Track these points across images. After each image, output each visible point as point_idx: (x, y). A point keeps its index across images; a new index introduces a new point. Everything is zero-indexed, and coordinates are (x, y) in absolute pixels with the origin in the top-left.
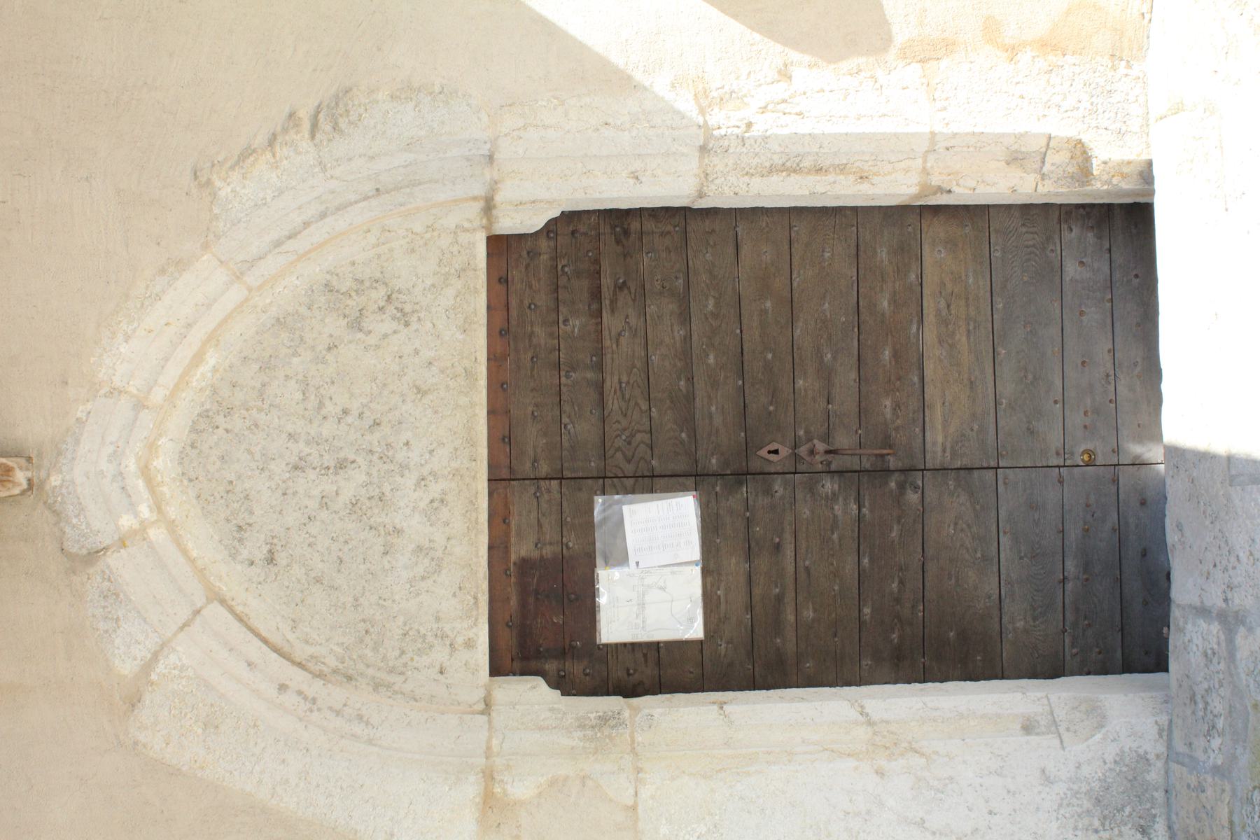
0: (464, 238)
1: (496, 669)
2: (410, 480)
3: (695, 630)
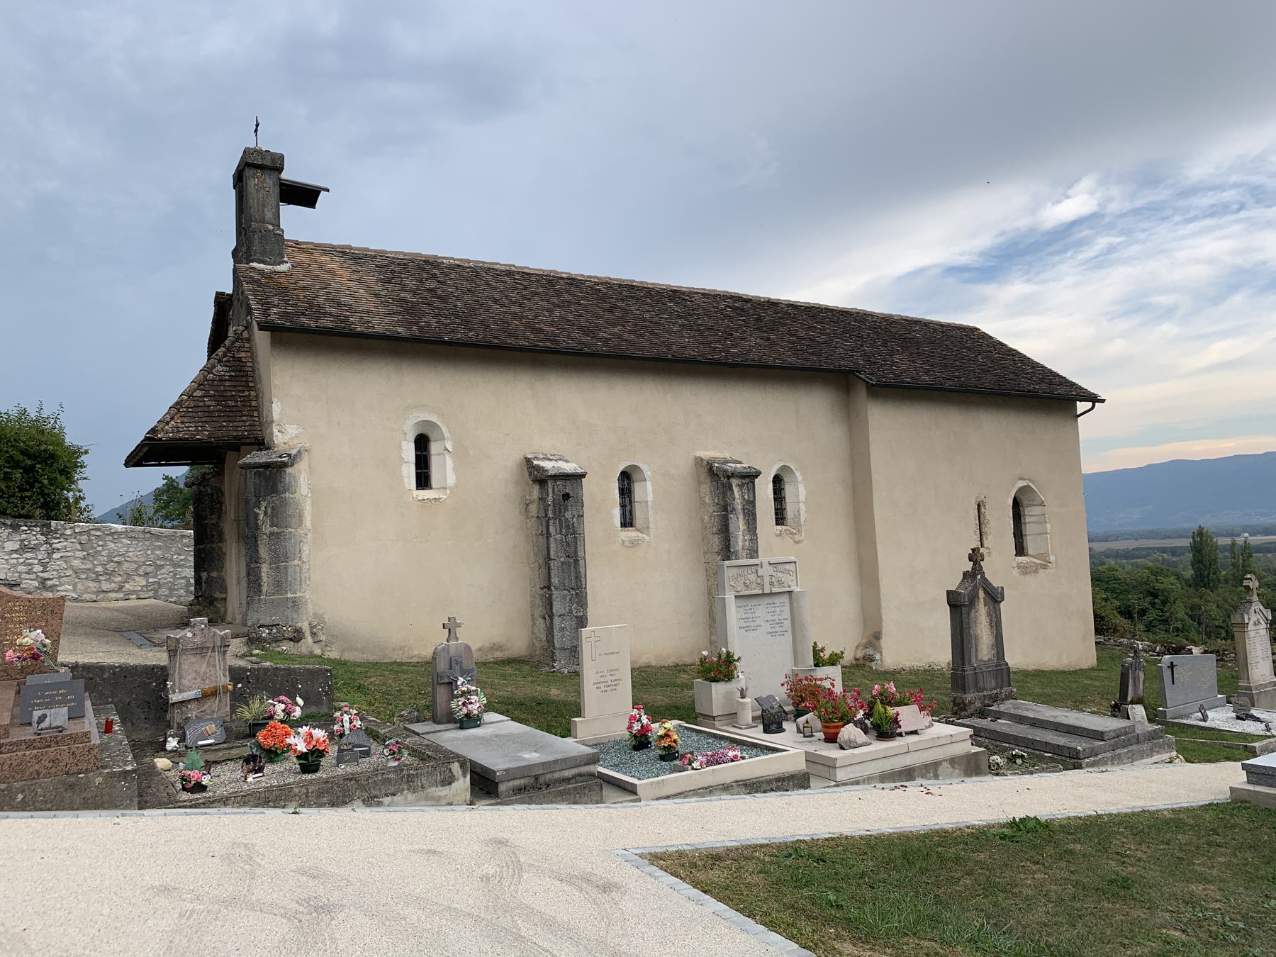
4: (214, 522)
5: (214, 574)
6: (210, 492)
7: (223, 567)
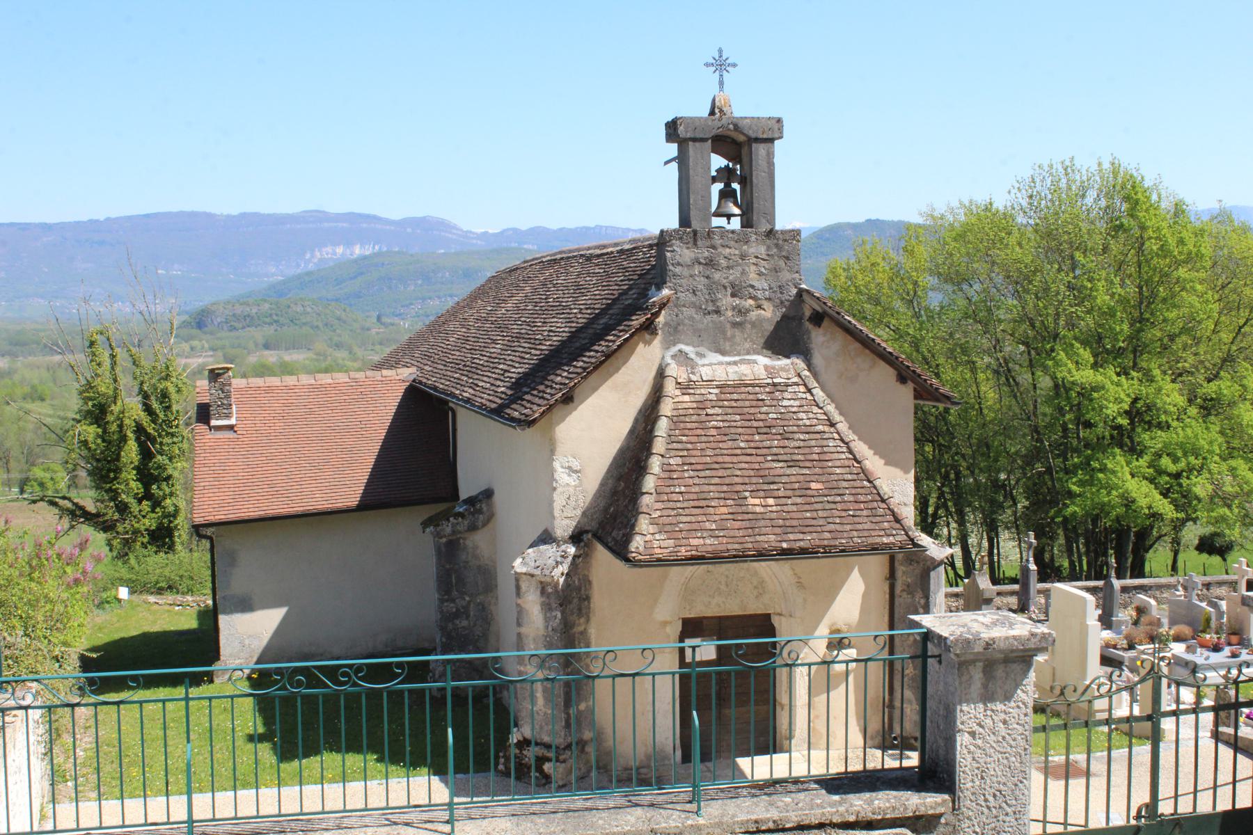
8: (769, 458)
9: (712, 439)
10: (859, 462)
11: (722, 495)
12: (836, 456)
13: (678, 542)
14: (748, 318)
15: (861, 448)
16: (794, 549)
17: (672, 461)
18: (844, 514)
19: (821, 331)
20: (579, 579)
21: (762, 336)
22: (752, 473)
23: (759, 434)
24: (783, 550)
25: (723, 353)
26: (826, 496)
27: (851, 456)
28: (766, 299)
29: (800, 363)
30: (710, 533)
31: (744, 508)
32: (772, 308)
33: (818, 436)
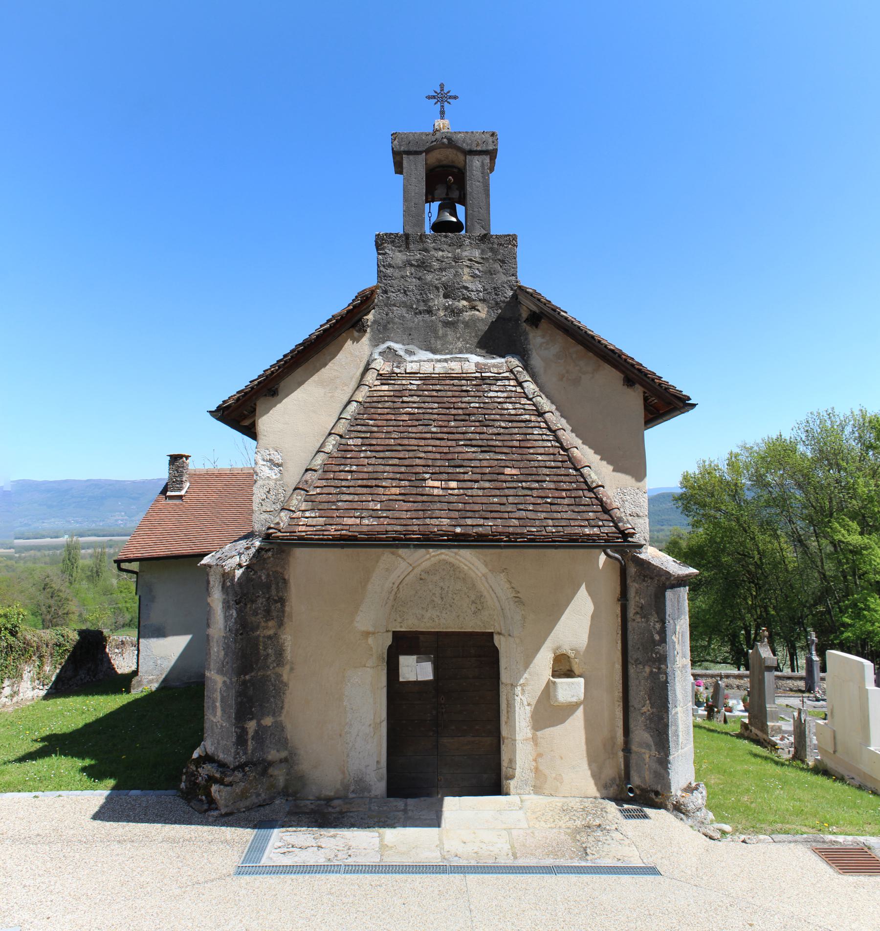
0: (492, 627)
1: (394, 632)
2: (438, 614)
3: (401, 680)
4: (271, 632)
5: (268, 721)
6: (264, 581)
7: (282, 708)
8: (461, 443)
9: (401, 423)
10: (565, 450)
11: (398, 476)
12: (540, 443)
13: (330, 521)
14: (461, 318)
15: (569, 437)
16: (470, 535)
17: (350, 442)
18: (539, 501)
19: (539, 332)
20: (268, 576)
21: (476, 336)
22: (438, 456)
23: (455, 420)
24: (457, 535)
25: (434, 351)
26: (521, 482)
27: (557, 444)
28: (480, 300)
29: (514, 362)
30: (371, 512)
31: (420, 490)
32: (486, 309)
33: (523, 424)
